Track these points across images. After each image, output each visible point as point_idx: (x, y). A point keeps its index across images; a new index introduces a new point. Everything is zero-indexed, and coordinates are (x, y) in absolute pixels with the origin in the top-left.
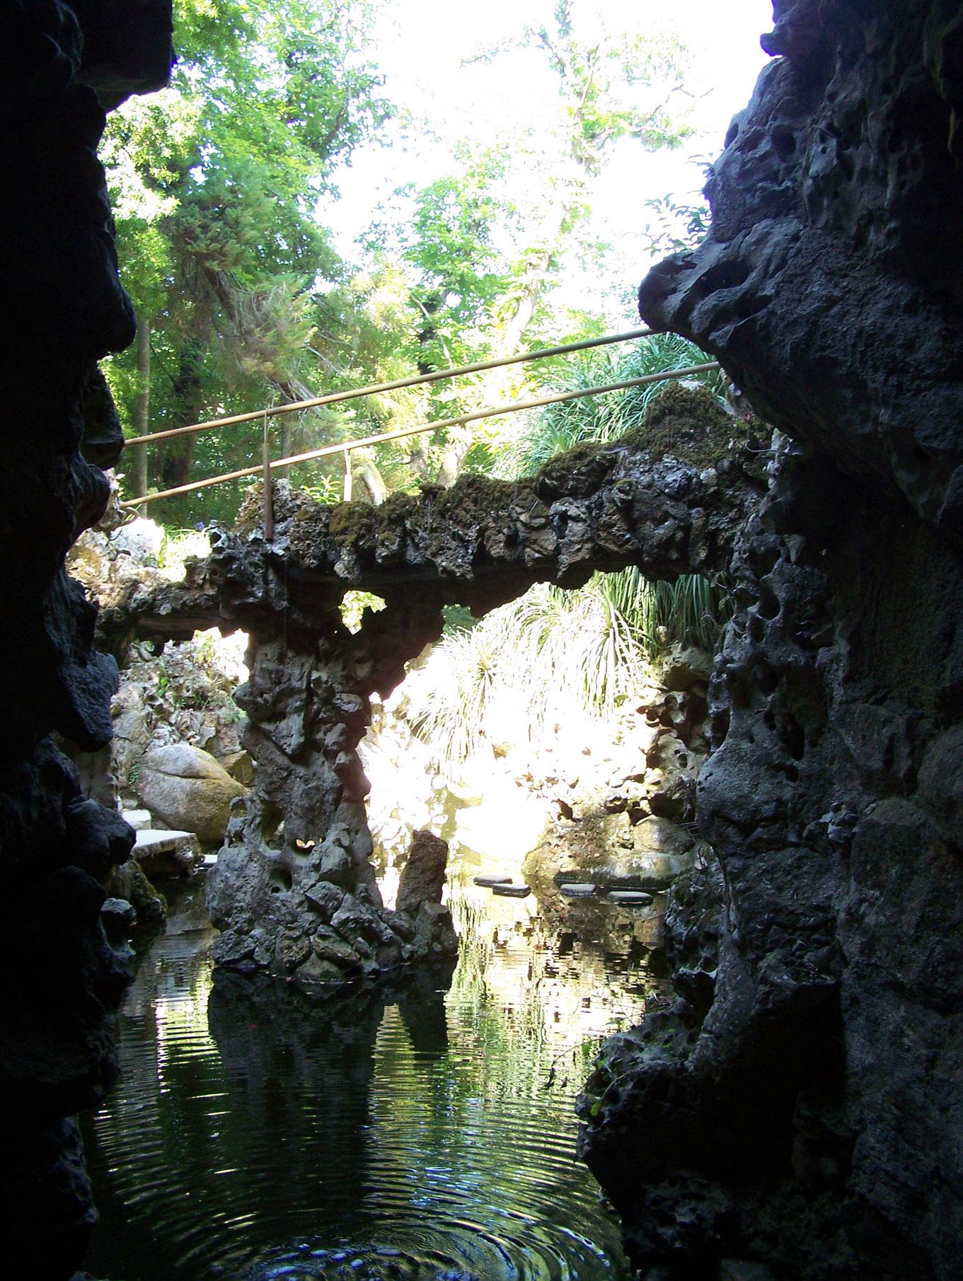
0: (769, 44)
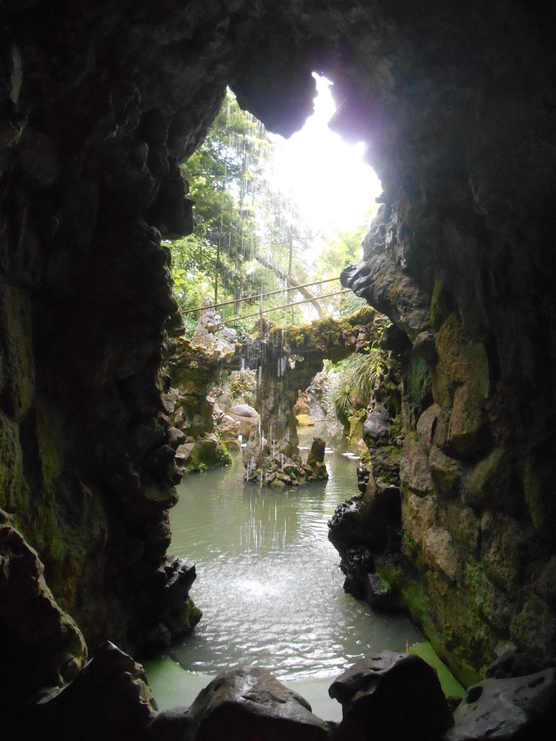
0: (378, 200)
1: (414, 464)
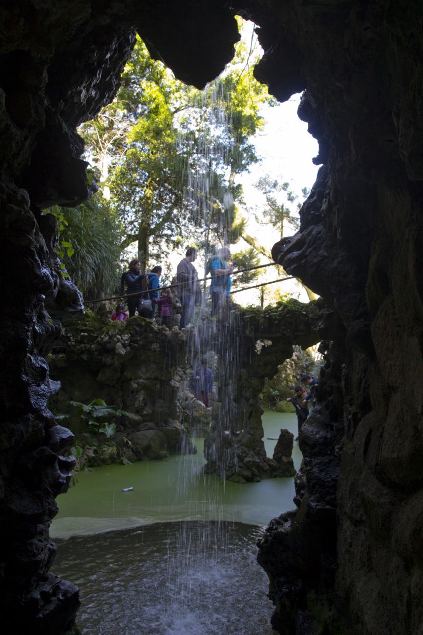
0: (316, 161)
1: (349, 483)
